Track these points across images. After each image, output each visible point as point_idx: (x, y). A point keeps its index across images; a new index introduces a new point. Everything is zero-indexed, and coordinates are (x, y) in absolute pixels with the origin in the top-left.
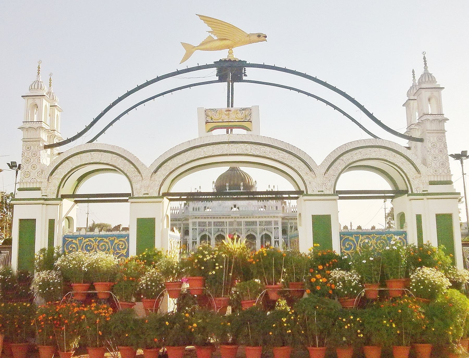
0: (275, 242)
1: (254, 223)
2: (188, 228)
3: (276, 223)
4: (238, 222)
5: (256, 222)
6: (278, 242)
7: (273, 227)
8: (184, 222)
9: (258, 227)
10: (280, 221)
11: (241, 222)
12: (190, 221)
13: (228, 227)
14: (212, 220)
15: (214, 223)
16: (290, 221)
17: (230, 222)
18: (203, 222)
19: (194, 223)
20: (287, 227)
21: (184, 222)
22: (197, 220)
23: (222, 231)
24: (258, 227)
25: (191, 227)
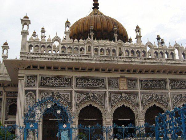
1: (160, 83)
2: (16, 100)
4: (129, 80)
5: (165, 81)
8: (9, 89)
9: (169, 91)
11: (135, 80)
12: (22, 74)
13: (107, 90)
14: (74, 75)
15: (77, 79)
18: (50, 78)
19: (30, 80)
21: (9, 89)
22: (38, 73)
23: (94, 97)
25: (22, 88)
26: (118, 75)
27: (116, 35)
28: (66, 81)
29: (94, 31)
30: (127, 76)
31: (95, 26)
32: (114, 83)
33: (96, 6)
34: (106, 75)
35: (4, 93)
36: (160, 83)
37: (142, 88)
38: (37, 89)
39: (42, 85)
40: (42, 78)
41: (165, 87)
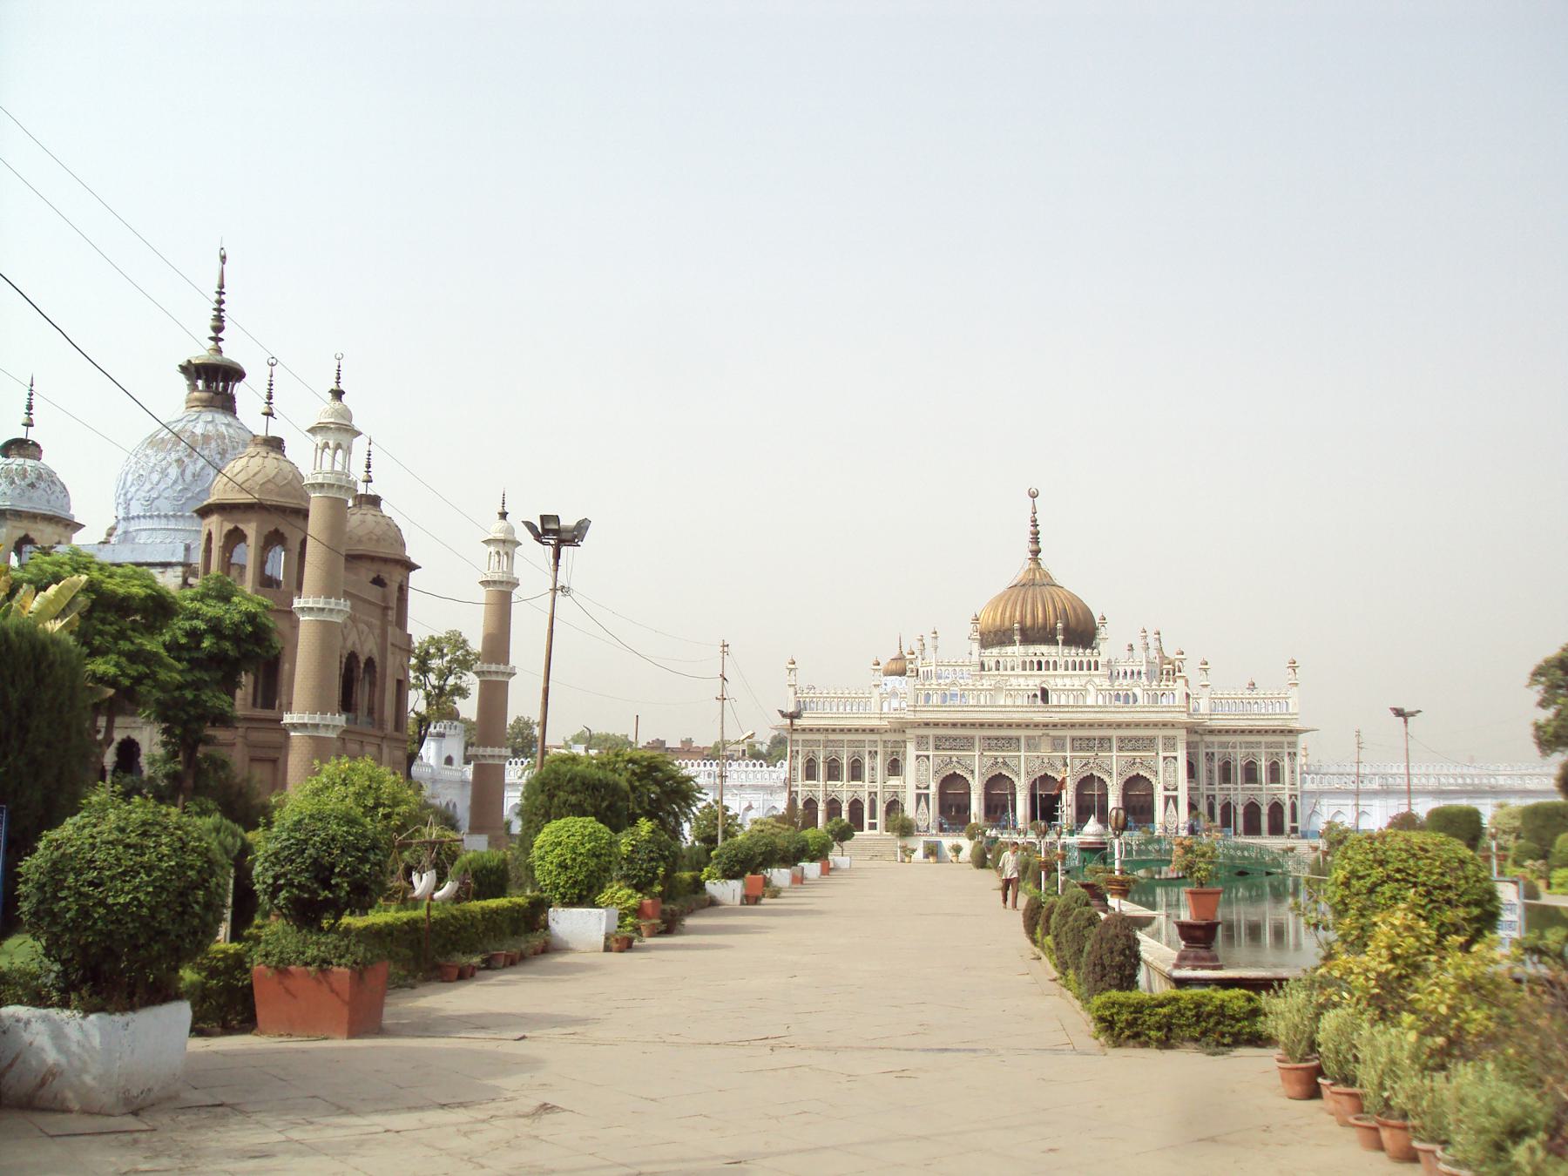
0: (1167, 799)
3: (1170, 743)
4: (1055, 738)
6: (1175, 799)
7: (1162, 754)
9: (1115, 753)
10: (1181, 735)
11: (1063, 738)
12: (910, 733)
14: (977, 733)
16: (1208, 738)
17: (1028, 738)
18: (947, 738)
19: (921, 742)
20: (1196, 754)
22: (931, 732)
23: (1005, 763)
24: (1115, 753)
25: (911, 751)
26: (1039, 733)
27: (1060, 638)
28: (968, 743)
29: (1023, 630)
30: (1052, 733)
31: (1021, 623)
32: (1032, 744)
33: (1036, 552)
34: (1022, 733)
35: (880, 745)
36: (1104, 743)
37: (1073, 749)
38: (930, 753)
39: (937, 748)
40: (937, 738)
41: (1110, 750)
